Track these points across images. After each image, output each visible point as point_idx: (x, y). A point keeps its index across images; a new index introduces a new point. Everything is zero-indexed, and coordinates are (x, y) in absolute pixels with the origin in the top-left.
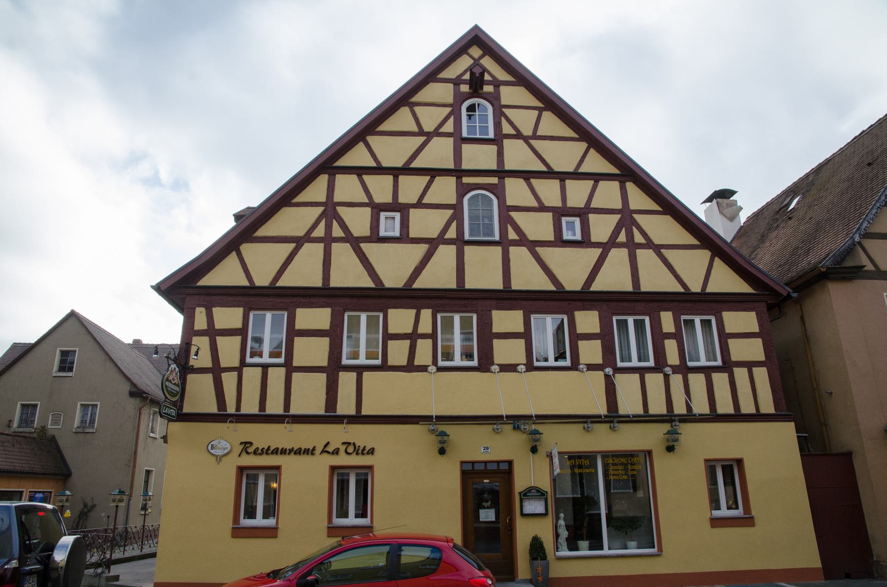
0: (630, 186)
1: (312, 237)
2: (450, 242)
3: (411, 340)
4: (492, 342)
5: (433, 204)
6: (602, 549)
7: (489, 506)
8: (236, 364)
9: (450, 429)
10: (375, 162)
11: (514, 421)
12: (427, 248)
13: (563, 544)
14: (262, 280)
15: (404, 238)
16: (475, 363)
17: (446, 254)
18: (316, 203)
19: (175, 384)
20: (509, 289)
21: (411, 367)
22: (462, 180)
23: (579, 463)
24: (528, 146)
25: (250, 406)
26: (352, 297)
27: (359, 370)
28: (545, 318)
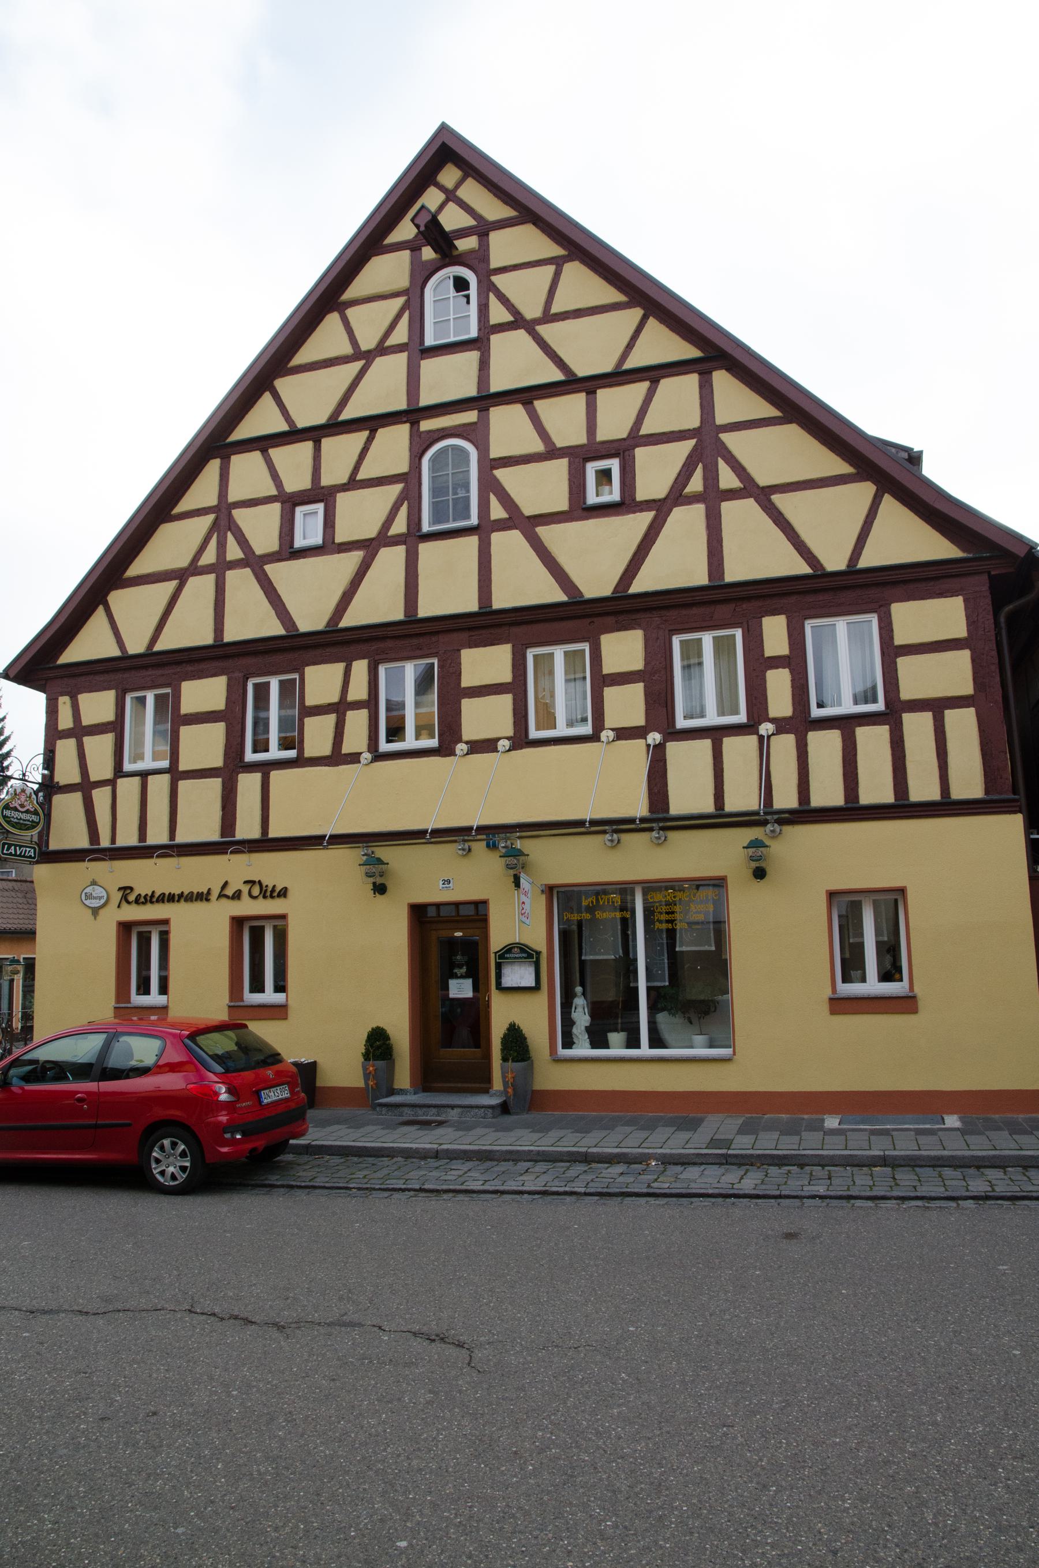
0: (721, 379)
1: (201, 566)
2: (396, 541)
3: (337, 713)
4: (460, 703)
5: (373, 479)
6: (638, 1046)
7: (464, 974)
8: (108, 774)
9: (383, 852)
10: (287, 422)
11: (486, 834)
12: (361, 558)
13: (580, 1037)
14: (136, 646)
15: (329, 546)
16: (433, 743)
17: (390, 560)
18: (204, 508)
19: (27, 812)
20: (488, 610)
21: (337, 758)
22: (419, 426)
23: (604, 902)
24: (534, 338)
25: (128, 837)
26: (255, 653)
27: (265, 768)
28: (835, 624)
